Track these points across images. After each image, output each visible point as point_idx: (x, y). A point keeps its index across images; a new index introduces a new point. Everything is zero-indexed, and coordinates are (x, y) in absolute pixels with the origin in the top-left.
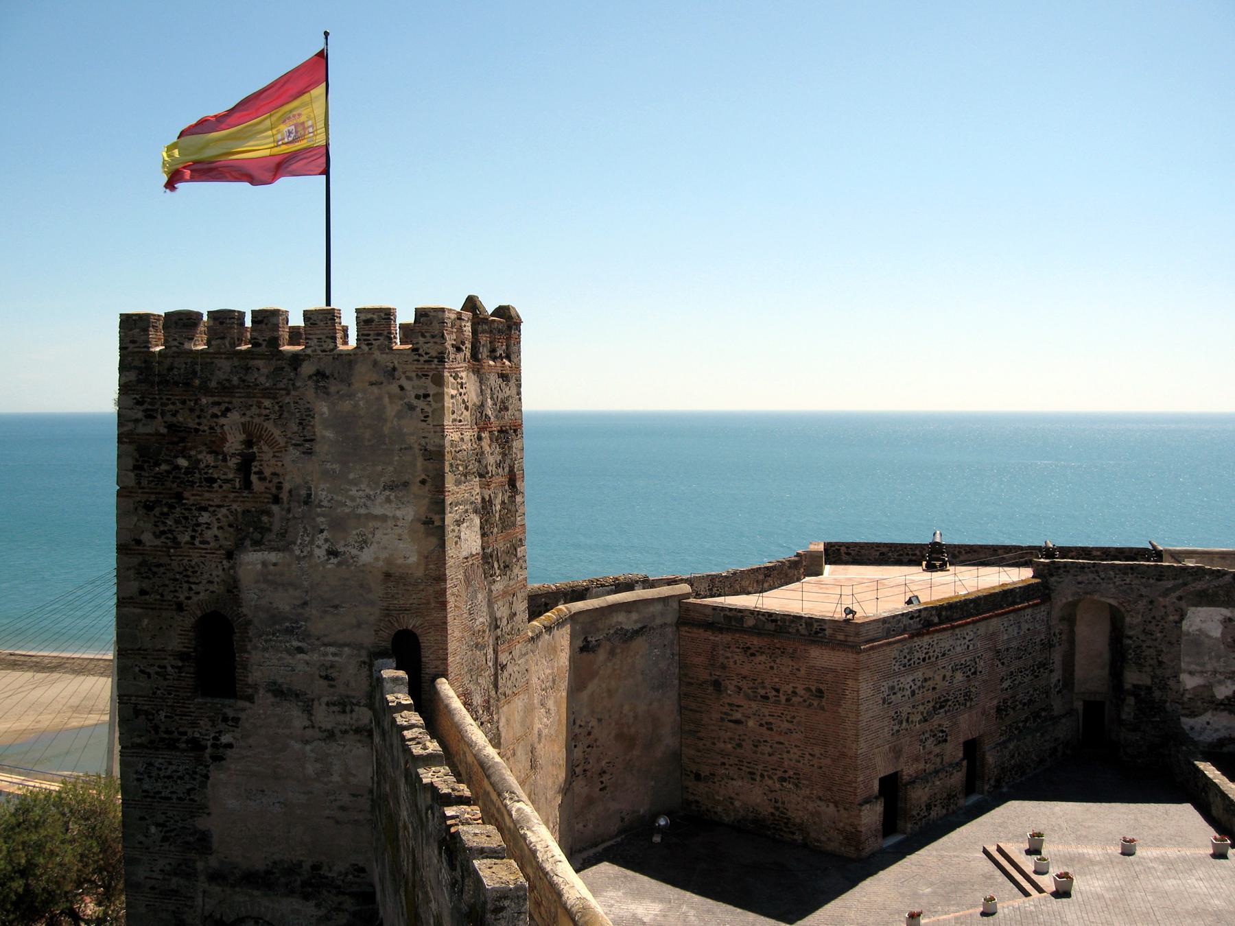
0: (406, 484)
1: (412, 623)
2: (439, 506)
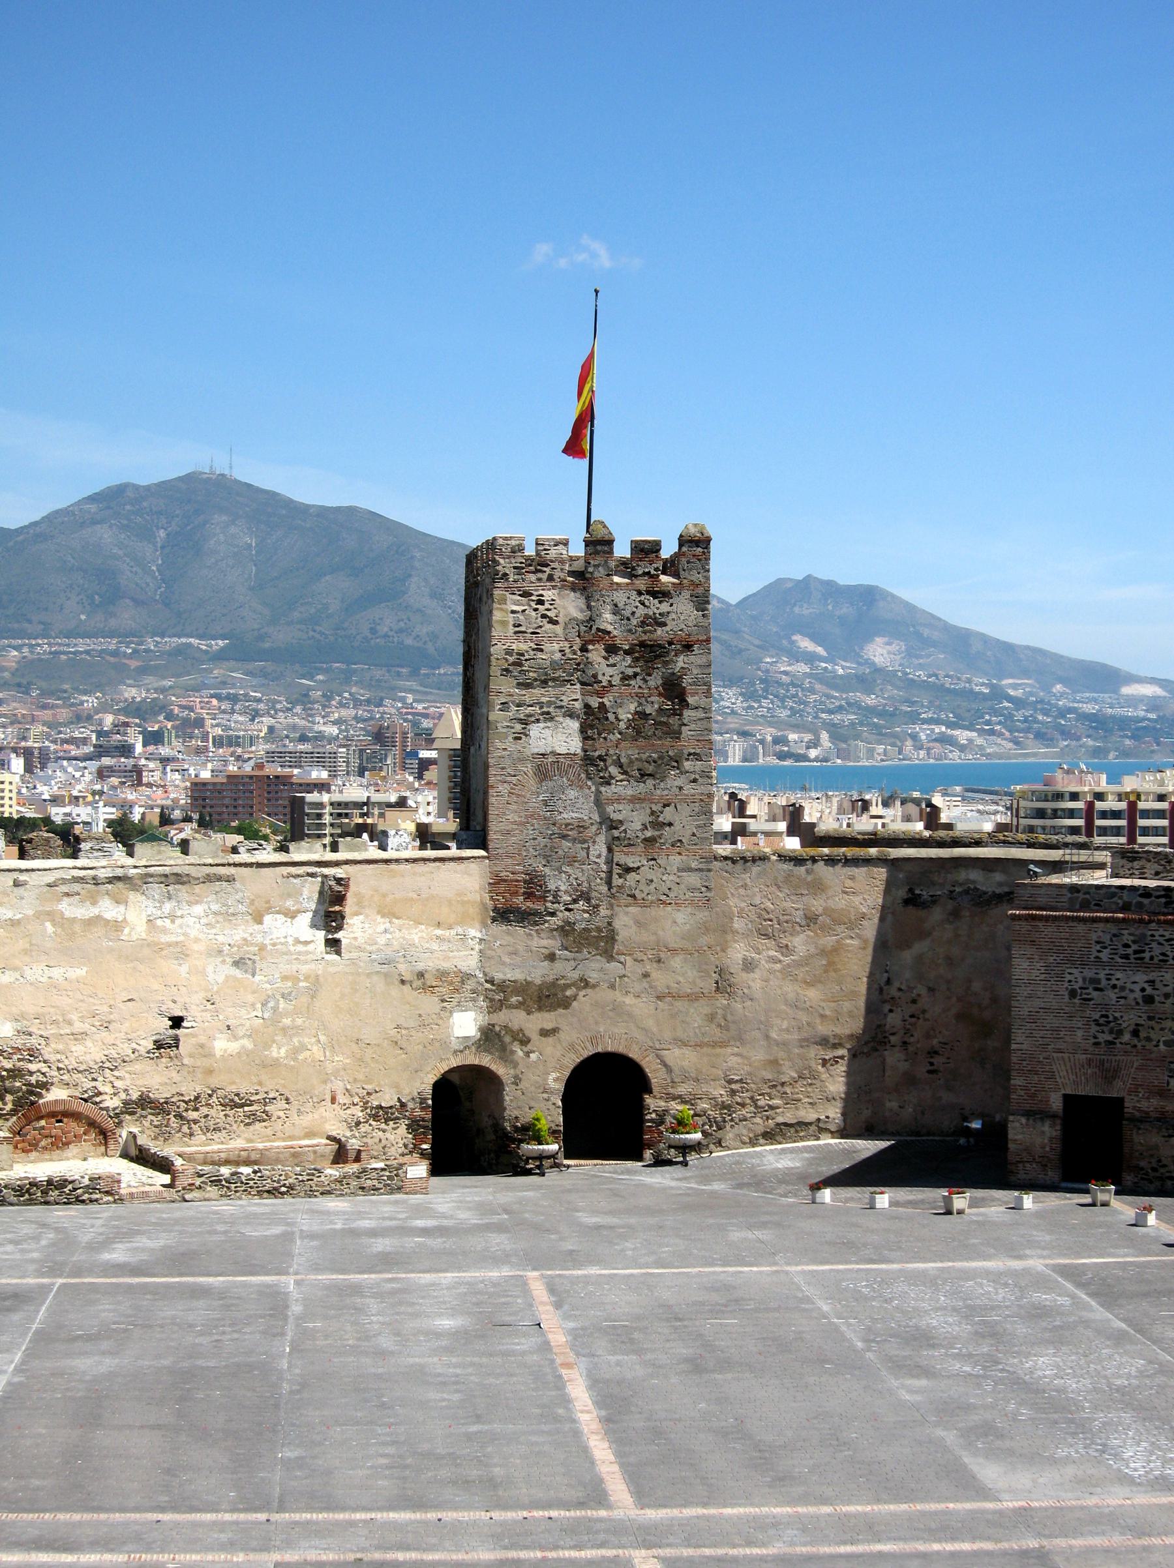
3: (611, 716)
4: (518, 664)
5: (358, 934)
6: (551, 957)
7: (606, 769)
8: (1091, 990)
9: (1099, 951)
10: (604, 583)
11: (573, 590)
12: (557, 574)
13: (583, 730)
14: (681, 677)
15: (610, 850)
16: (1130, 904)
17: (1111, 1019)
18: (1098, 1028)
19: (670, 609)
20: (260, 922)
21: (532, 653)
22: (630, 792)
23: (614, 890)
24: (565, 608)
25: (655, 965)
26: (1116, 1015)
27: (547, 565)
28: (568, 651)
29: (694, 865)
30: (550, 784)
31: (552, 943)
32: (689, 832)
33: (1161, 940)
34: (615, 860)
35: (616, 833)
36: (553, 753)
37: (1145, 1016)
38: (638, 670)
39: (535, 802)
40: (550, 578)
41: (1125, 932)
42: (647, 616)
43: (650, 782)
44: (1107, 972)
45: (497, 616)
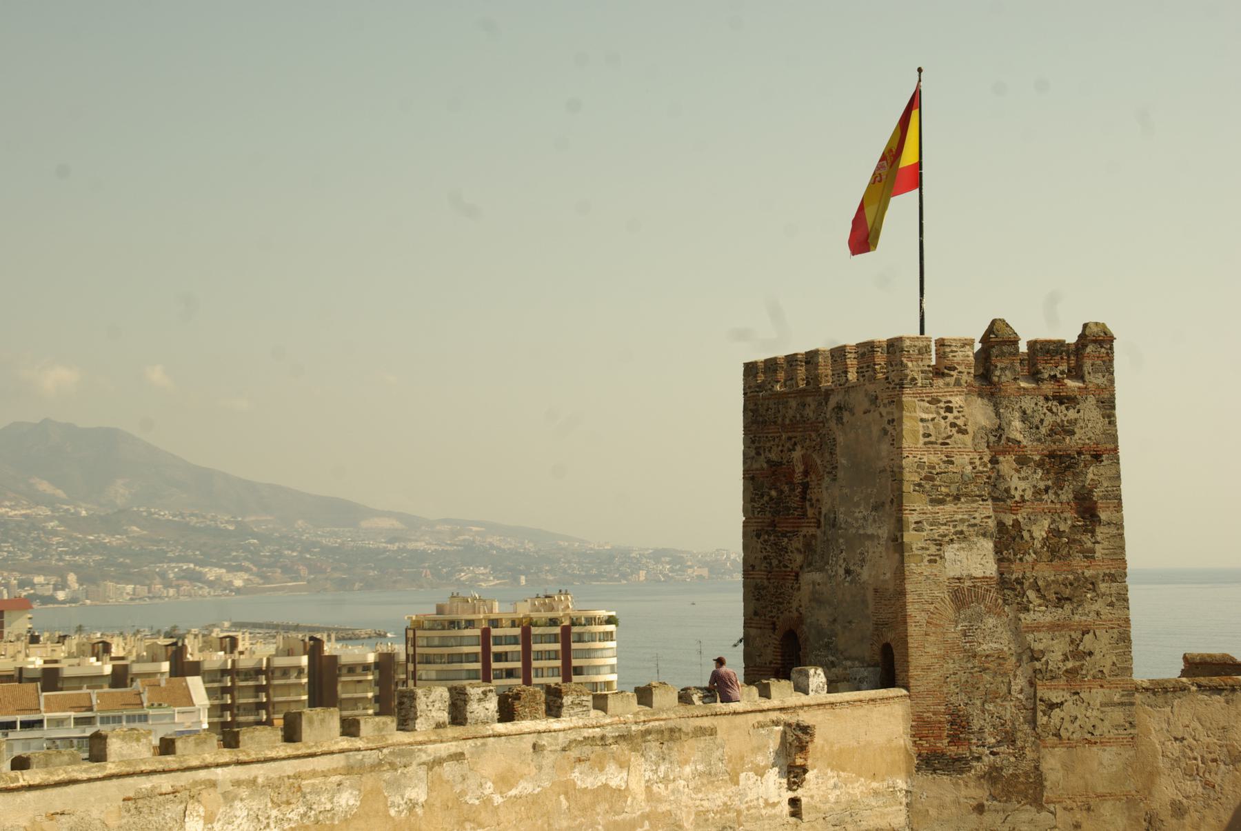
0: (883, 504)
1: (890, 637)
2: (900, 524)
3: (1026, 535)
4: (929, 478)
5: (814, 792)
6: (980, 809)
7: (1024, 594)
10: (1011, 388)
11: (980, 395)
12: (965, 377)
13: (998, 550)
14: (1091, 491)
15: (1032, 684)
19: (1077, 416)
20: (737, 783)
21: (943, 466)
22: (1048, 618)
23: (1039, 730)
24: (971, 414)
25: (1084, 813)
27: (955, 369)
28: (977, 462)
29: (1116, 698)
30: (969, 612)
31: (980, 793)
32: (1108, 664)
34: (1039, 695)
35: (1038, 665)
36: (971, 578)
38: (1050, 483)
39: (954, 632)
40: (958, 383)
42: (1055, 424)
43: (1068, 607)
45: (907, 425)
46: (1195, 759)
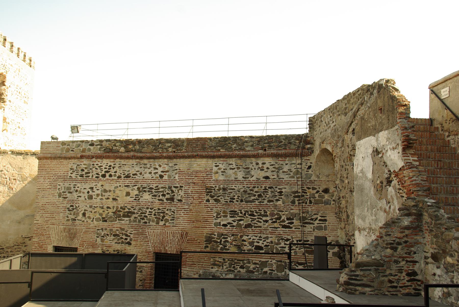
8: (67, 193)
9: (71, 173)
16: (85, 149)
17: (74, 207)
18: (69, 212)
26: (77, 205)
33: (97, 167)
37: (88, 206)
41: (82, 163)
44: (74, 184)
46: (6, 178)
